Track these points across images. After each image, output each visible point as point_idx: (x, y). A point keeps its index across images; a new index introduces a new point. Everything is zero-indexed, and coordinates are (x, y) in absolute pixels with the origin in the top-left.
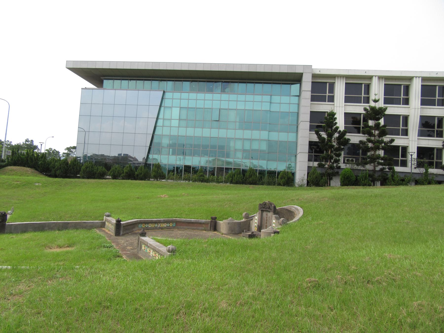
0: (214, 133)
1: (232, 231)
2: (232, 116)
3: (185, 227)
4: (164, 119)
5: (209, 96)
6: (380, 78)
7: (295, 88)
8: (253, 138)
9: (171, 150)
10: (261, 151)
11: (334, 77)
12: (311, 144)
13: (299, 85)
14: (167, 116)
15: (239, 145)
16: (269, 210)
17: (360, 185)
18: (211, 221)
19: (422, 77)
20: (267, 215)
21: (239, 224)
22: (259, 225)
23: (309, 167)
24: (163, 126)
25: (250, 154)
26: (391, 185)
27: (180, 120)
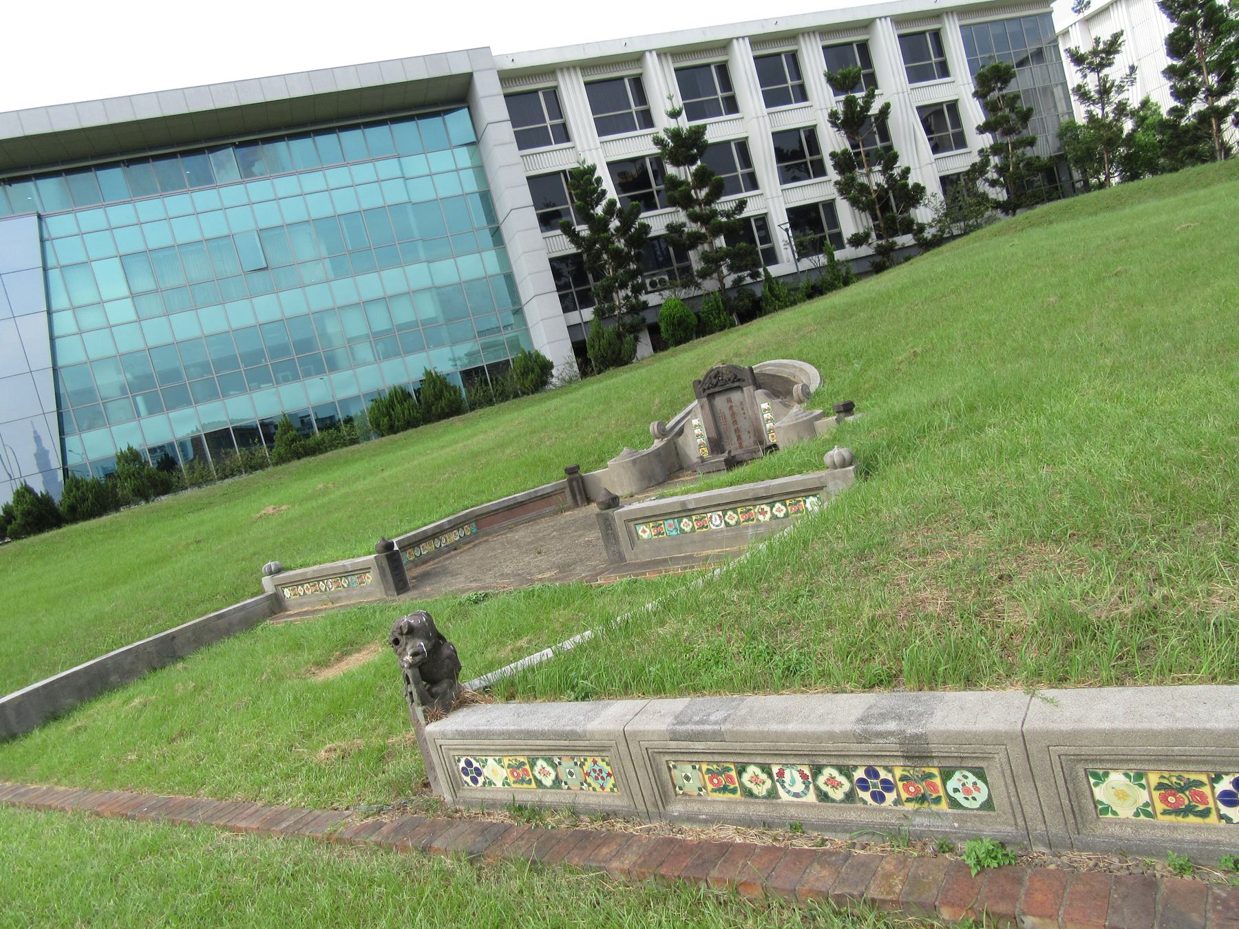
0: (266, 308)
1: (650, 480)
3: (505, 524)
4: (74, 308)
5: (205, 198)
6: (662, 53)
7: (458, 121)
8: (390, 292)
9: (139, 399)
10: (428, 324)
11: (550, 71)
12: (557, 265)
13: (466, 111)
14: (84, 294)
15: (355, 325)
16: (736, 384)
17: (711, 332)
18: (570, 481)
19: (749, 37)
20: (729, 401)
21: (657, 453)
22: (714, 435)
23: (570, 328)
24: (80, 332)
25: (393, 342)
26: (775, 310)
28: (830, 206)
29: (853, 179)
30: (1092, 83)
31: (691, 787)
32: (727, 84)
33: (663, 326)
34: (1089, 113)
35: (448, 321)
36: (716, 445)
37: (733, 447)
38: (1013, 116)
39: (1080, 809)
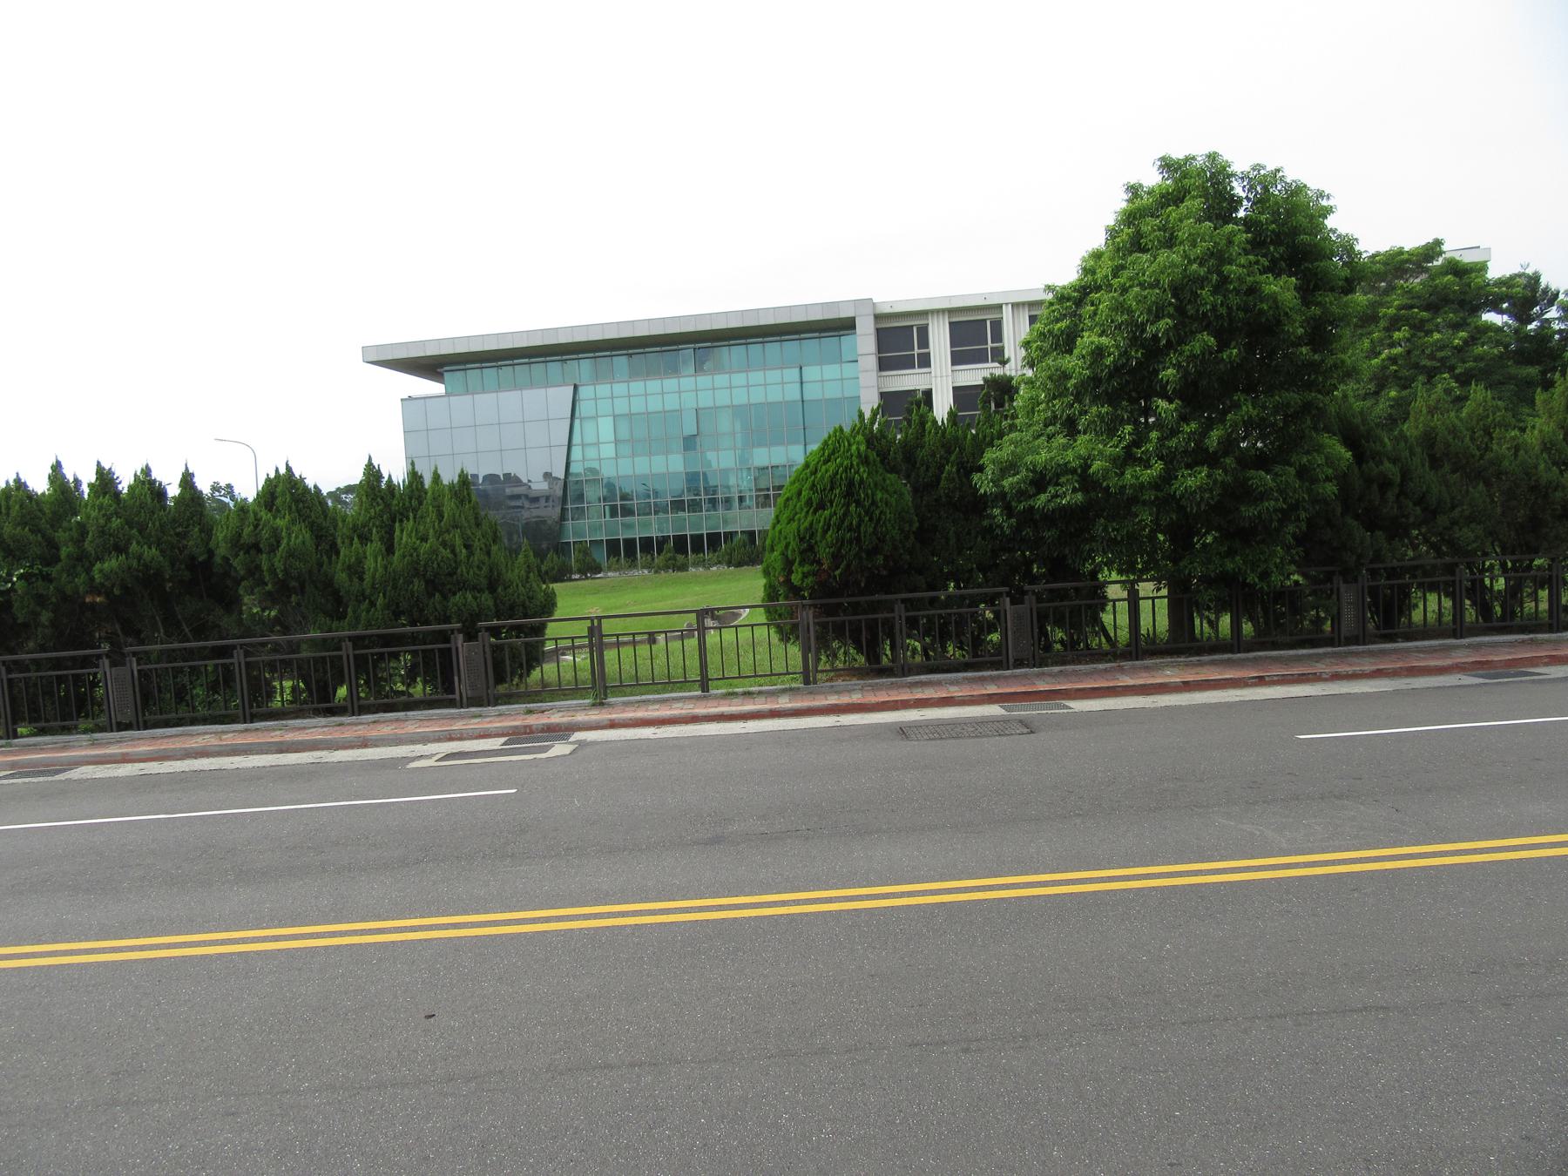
2: (725, 423)
4: (583, 445)
5: (671, 383)
6: (1015, 306)
11: (924, 314)
14: (590, 438)
27: (616, 442)
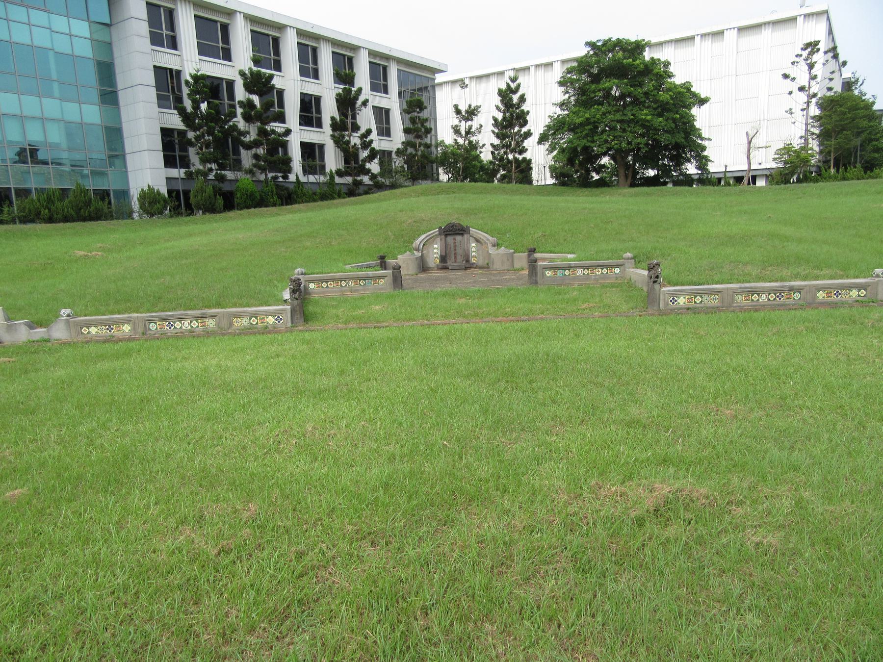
6: (247, 17)
20: (455, 239)
28: (322, 147)
29: (343, 136)
30: (463, 126)
31: (739, 300)
32: (277, 52)
33: (239, 195)
34: (456, 142)
35: (70, 149)
36: (443, 259)
37: (449, 263)
38: (423, 130)
39: (815, 297)
